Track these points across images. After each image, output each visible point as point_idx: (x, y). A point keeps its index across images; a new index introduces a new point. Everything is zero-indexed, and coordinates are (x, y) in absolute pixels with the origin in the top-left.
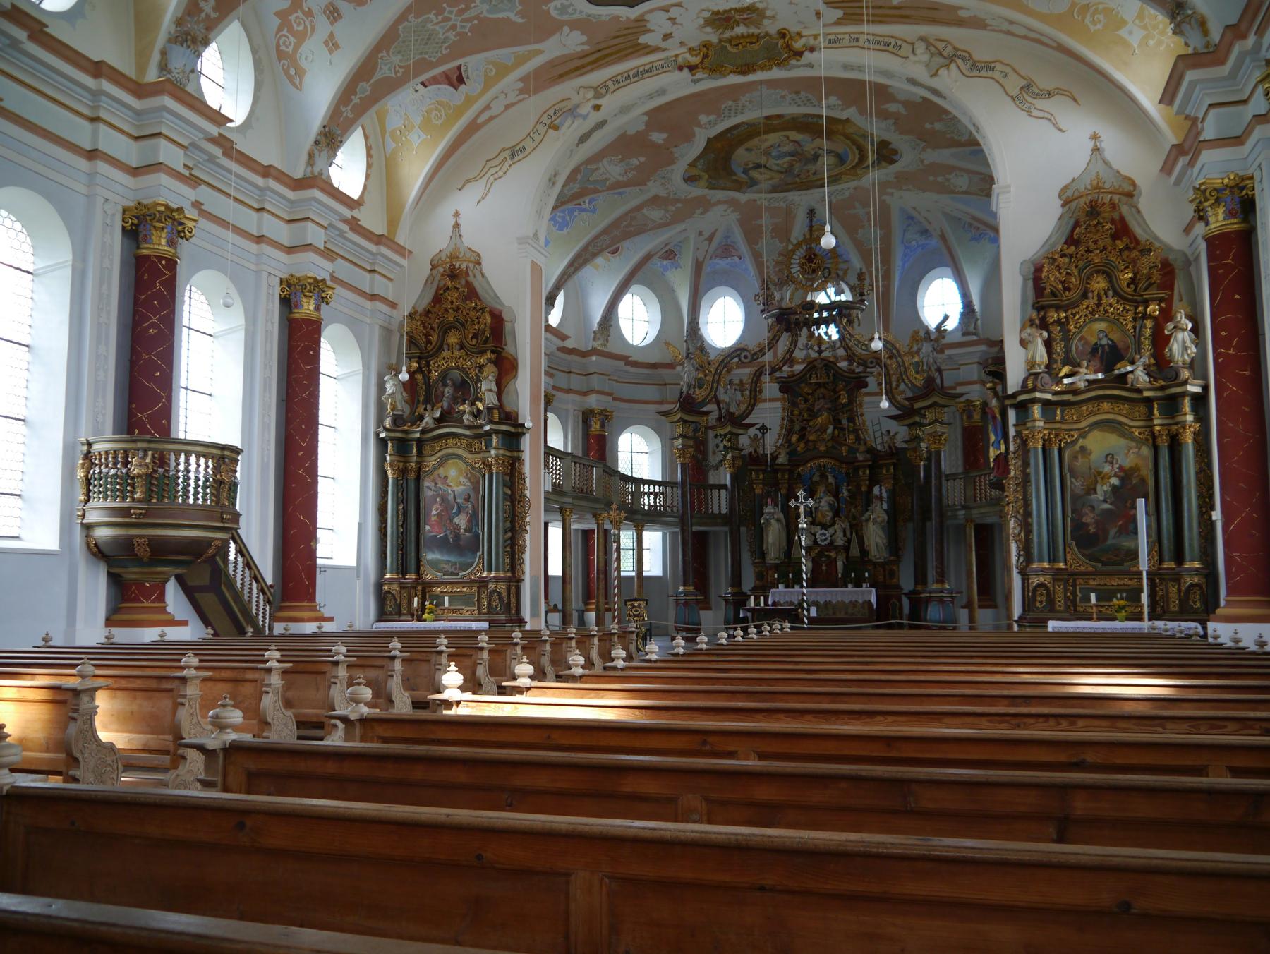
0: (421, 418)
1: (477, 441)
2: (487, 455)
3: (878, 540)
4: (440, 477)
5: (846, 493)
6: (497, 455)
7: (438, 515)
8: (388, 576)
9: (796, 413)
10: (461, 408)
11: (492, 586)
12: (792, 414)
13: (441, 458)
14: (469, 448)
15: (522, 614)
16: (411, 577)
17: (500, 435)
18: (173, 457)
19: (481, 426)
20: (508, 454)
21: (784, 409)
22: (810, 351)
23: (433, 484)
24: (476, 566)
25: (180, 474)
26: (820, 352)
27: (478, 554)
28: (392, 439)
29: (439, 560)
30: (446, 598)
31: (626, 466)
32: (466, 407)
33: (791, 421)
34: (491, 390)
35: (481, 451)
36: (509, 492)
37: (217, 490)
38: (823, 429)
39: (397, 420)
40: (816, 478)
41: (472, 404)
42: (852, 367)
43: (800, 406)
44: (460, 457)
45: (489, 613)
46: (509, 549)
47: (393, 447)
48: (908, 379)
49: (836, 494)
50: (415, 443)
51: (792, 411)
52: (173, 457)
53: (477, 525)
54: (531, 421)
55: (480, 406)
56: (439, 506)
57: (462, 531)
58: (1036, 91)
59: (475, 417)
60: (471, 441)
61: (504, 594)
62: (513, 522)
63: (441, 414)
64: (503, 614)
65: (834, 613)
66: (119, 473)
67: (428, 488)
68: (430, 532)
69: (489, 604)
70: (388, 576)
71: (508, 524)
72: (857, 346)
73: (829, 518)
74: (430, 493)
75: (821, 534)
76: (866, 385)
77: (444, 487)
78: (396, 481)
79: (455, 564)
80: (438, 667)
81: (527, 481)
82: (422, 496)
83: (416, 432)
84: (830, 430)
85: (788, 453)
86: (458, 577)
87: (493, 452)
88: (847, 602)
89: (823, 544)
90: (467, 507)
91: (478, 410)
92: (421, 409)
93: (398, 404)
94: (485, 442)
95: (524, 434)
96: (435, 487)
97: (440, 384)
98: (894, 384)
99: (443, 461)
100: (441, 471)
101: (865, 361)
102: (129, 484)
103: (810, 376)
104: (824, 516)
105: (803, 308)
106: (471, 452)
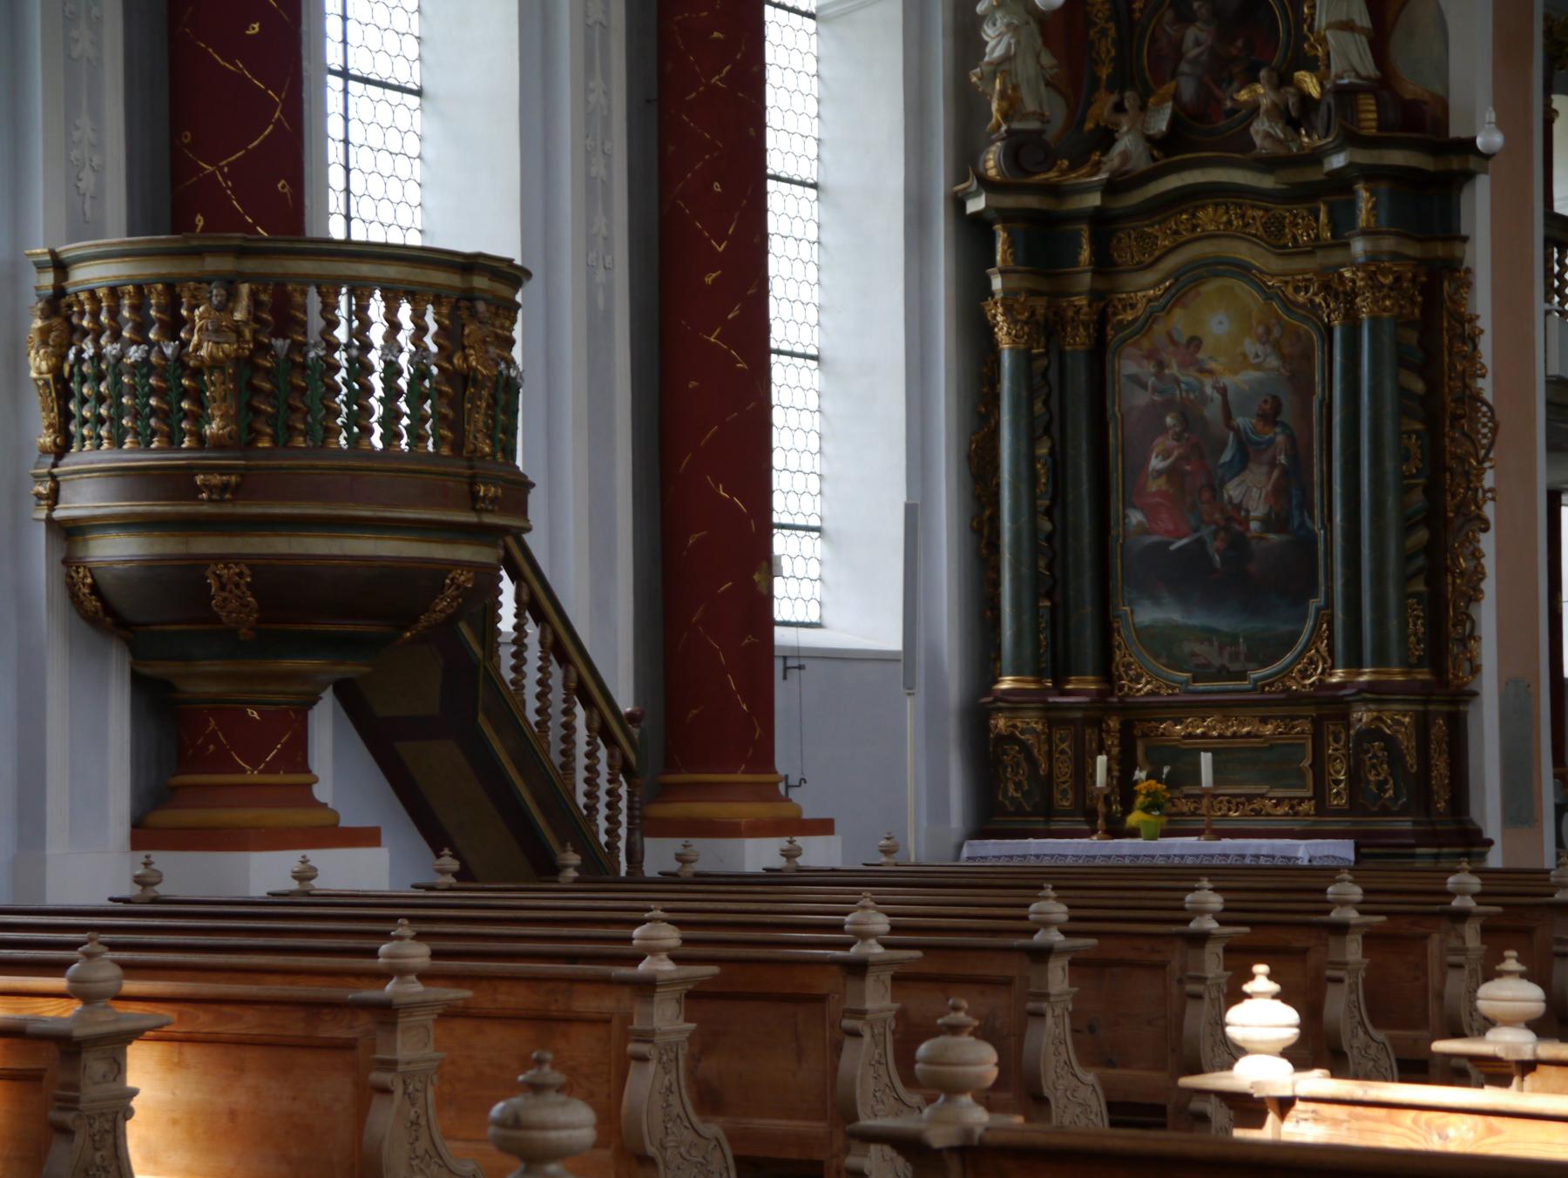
0: (1106, 138)
1: (1301, 210)
2: (1337, 256)
4: (1174, 342)
6: (1373, 257)
7: (1172, 473)
8: (1007, 683)
10: (1244, 96)
11: (1362, 716)
13: (1177, 275)
14: (1274, 237)
15: (1474, 813)
16: (1084, 685)
17: (1383, 187)
18: (314, 301)
19: (1315, 158)
20: (1412, 250)
23: (1150, 368)
24: (1306, 648)
25: (340, 356)
27: (1314, 604)
28: (1007, 217)
29: (1177, 626)
30: (1206, 759)
32: (1262, 93)
34: (1347, 26)
35: (1316, 246)
36: (1419, 386)
37: (456, 403)
39: (1020, 150)
41: (1283, 80)
44: (1242, 270)
45: (1355, 808)
46: (1420, 586)
47: (1011, 243)
50: (1085, 231)
52: (314, 301)
53: (1306, 505)
54: (1501, 125)
55: (1311, 84)
56: (1170, 443)
57: (1254, 525)
59: (1293, 124)
60: (1279, 210)
61: (1407, 743)
62: (1434, 491)
63: (1174, 121)
64: (1403, 812)
66: (153, 359)
67: (1137, 381)
68: (1143, 530)
69: (1355, 777)
70: (1007, 683)
71: (1417, 499)
74: (1141, 399)
77: (1188, 377)
78: (1025, 359)
79: (1234, 639)
80: (1191, 988)
81: (1485, 346)
82: (1114, 410)
83: (1088, 189)
86: (1246, 685)
87: (1359, 247)
90: (1271, 442)
91: (1305, 98)
92: (1103, 106)
93: (1025, 93)
94: (1330, 213)
95: (1469, 176)
96: (1159, 375)
97: (1169, 15)
99: (1185, 284)
100: (1179, 322)
102: (185, 393)
106: (1280, 250)
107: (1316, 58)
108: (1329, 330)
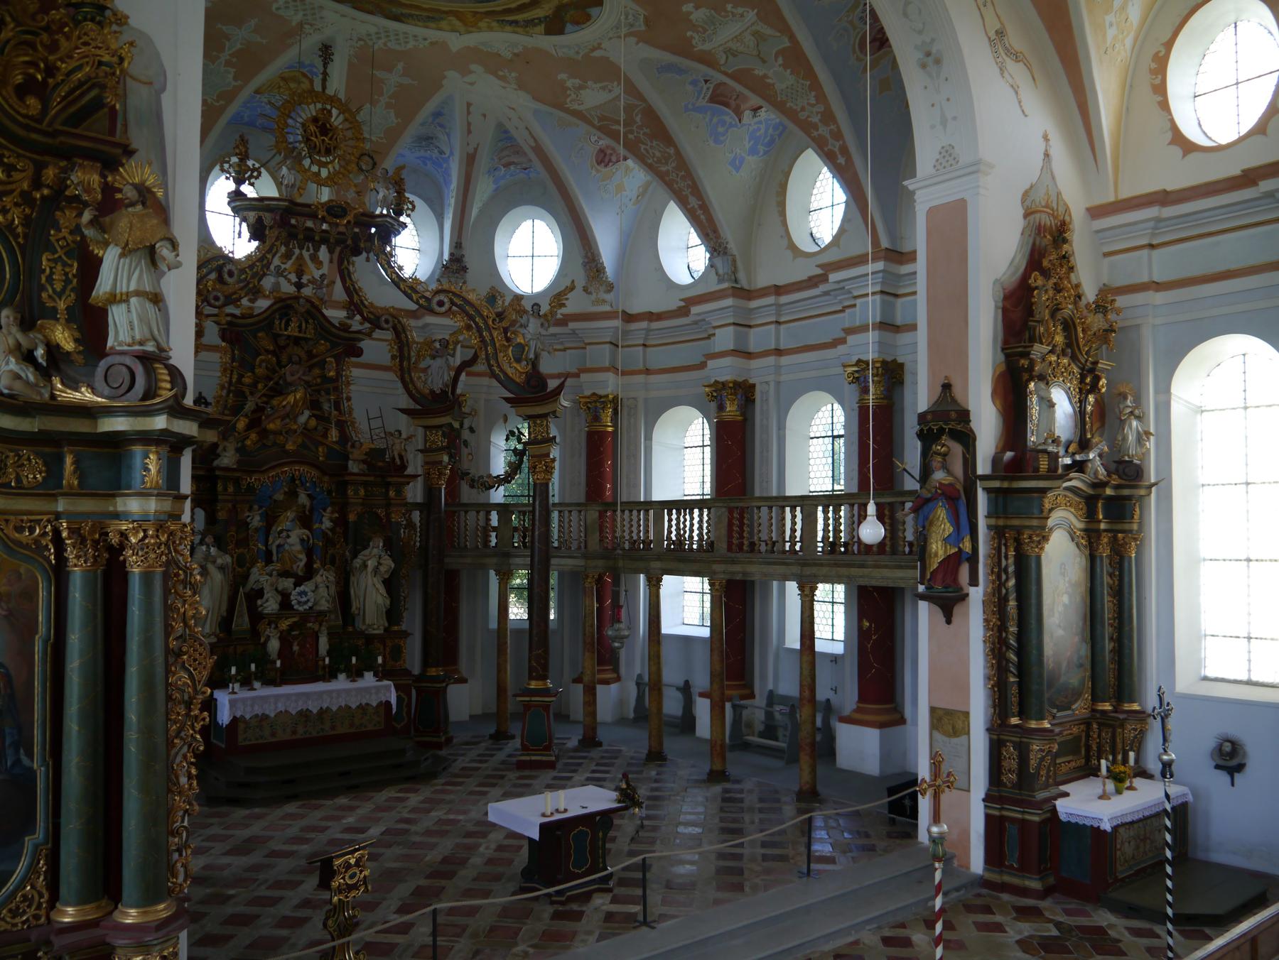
3: (380, 600)
5: (327, 524)
9: (247, 380)
12: (239, 381)
21: (225, 370)
22: (282, 280)
24: (21, 886)
26: (299, 286)
27: (29, 842)
31: (824, 622)
33: (241, 395)
38: (292, 415)
40: (279, 497)
42: (349, 322)
43: (257, 371)
48: (499, 366)
49: (305, 520)
51: (241, 376)
55: (64, 338)
58: (1007, 45)
59: (45, 373)
65: (333, 728)
72: (410, 298)
73: (302, 564)
75: (301, 594)
76: (359, 353)
84: (302, 419)
85: (237, 450)
88: (354, 706)
89: (301, 609)
91: (53, 350)
94: (76, 462)
98: (413, 360)
101: (378, 318)
103: (287, 325)
104: (294, 560)
105: (328, 212)
107: (55, 310)
108: (60, 573)
